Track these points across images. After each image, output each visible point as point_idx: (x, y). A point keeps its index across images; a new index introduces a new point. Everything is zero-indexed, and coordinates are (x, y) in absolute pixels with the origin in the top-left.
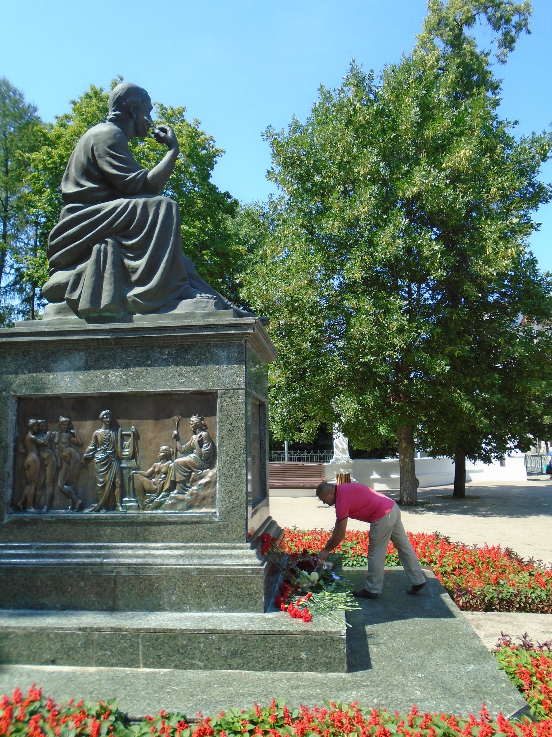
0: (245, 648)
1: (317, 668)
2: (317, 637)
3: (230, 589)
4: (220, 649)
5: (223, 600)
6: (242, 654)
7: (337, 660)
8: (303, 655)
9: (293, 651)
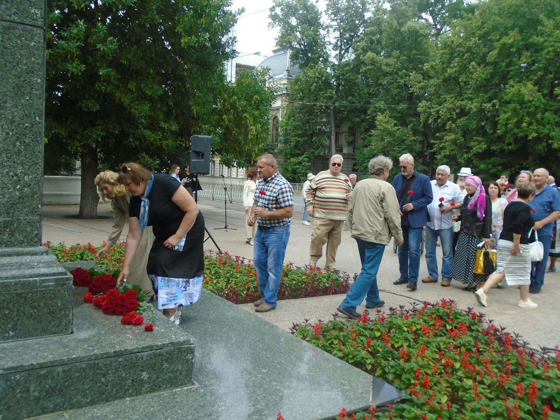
0: (66, 382)
1: (160, 387)
2: (163, 351)
3: (22, 309)
4: (28, 391)
5: (10, 326)
6: (62, 390)
7: (184, 373)
8: (145, 375)
9: (132, 373)
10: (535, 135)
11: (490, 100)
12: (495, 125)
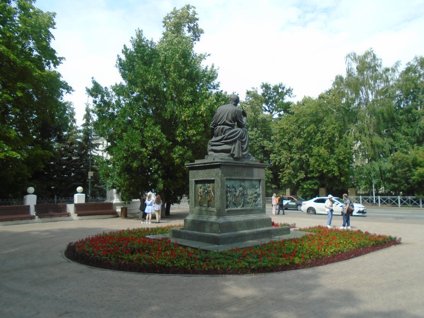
10: (326, 170)
11: (304, 153)
12: (308, 166)
